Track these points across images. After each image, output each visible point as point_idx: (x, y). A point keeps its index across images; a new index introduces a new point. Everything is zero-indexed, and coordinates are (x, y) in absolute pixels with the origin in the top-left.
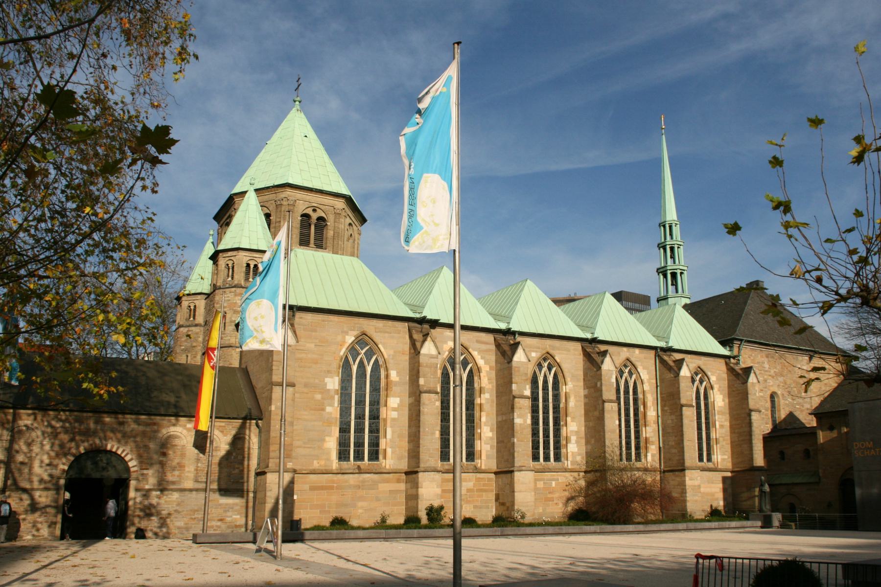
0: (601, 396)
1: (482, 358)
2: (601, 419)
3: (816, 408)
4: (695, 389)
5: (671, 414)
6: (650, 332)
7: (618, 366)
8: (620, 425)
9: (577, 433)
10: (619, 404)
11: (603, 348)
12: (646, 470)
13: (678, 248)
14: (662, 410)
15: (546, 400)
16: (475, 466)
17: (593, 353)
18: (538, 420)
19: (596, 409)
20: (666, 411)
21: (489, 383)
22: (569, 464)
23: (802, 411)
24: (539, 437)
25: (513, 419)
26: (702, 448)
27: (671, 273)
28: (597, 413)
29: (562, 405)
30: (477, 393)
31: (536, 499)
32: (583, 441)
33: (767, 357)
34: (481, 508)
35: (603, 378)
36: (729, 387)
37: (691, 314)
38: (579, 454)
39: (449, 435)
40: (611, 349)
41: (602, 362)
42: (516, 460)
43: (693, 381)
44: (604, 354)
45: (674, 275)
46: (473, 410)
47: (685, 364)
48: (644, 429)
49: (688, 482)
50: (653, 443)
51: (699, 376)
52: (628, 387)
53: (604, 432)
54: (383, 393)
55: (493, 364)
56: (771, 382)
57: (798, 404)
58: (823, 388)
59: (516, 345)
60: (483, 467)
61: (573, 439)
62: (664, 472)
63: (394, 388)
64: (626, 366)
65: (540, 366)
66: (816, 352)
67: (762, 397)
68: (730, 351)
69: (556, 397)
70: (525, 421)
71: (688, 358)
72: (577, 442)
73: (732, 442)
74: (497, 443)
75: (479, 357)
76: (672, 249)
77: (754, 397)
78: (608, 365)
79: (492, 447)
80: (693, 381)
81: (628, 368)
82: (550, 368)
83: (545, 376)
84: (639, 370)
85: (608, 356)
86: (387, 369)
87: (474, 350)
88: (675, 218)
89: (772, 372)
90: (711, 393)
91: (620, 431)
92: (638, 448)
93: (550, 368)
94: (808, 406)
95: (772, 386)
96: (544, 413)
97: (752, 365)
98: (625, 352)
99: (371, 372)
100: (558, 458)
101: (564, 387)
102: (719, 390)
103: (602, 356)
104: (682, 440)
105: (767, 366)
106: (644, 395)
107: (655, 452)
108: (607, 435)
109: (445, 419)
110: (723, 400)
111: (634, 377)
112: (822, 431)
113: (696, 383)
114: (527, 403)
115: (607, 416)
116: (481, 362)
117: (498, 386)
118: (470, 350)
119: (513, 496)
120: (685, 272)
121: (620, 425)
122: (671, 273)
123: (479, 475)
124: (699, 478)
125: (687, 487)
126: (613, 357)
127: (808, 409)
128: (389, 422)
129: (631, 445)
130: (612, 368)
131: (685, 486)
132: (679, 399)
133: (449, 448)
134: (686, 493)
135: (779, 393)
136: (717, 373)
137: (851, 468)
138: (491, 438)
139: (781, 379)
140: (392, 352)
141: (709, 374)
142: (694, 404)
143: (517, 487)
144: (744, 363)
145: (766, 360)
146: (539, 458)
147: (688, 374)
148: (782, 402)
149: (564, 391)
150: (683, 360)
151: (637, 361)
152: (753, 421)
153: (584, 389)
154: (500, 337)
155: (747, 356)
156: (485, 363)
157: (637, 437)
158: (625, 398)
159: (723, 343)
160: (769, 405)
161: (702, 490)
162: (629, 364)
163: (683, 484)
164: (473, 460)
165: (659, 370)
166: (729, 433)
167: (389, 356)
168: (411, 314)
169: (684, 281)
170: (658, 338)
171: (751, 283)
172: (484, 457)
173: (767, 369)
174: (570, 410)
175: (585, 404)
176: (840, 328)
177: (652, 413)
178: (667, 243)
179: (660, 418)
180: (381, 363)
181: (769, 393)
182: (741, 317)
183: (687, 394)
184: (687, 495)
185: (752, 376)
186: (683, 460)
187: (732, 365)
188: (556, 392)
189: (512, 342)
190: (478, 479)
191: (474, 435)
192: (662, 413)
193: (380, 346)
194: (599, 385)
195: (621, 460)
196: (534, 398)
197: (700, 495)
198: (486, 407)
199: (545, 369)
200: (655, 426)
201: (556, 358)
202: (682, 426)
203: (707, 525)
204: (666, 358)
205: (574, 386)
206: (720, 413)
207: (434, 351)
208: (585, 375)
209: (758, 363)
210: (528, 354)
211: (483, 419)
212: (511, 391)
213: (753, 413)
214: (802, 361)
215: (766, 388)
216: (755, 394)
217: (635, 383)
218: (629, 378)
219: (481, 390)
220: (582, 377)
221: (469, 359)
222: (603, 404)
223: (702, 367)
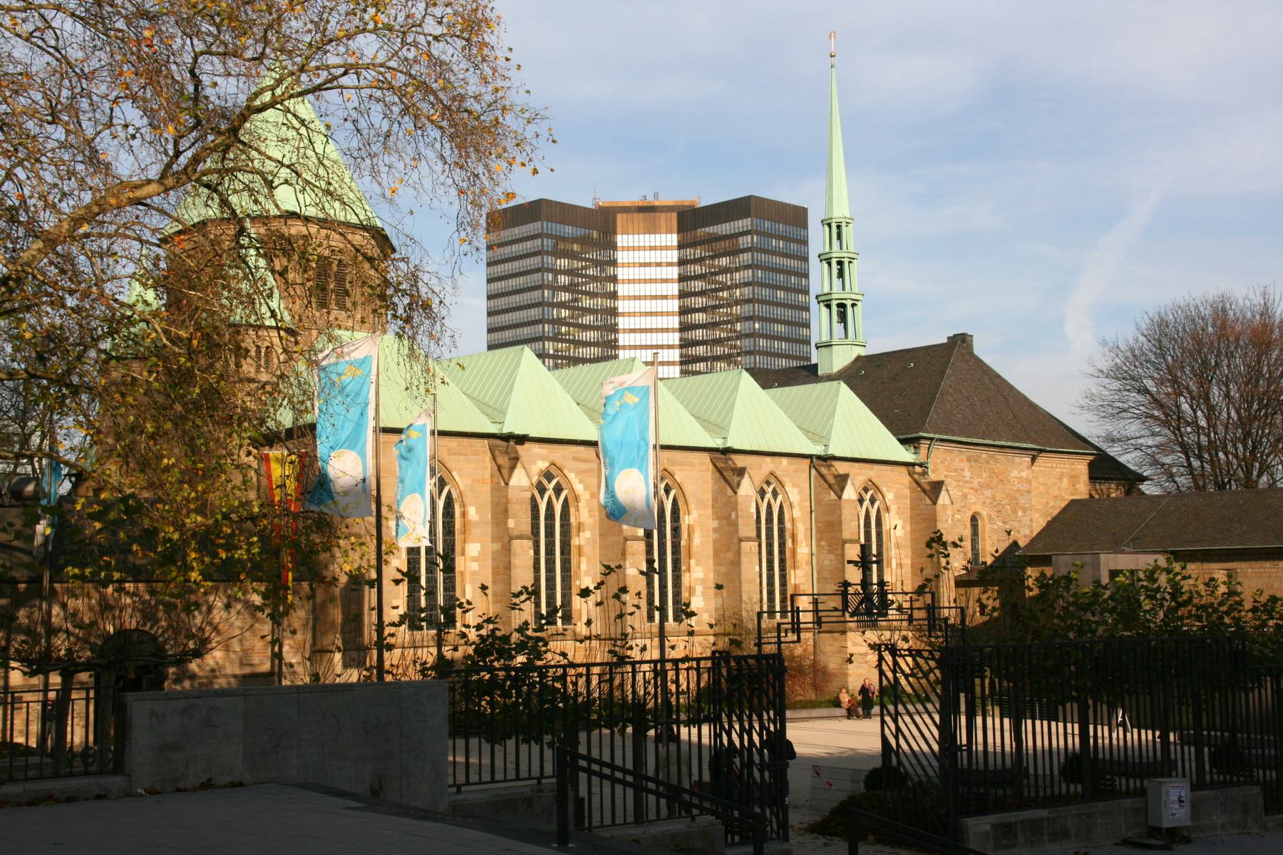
1: (581, 482)
5: (830, 552)
9: (703, 581)
14: (818, 545)
19: (729, 550)
20: (823, 547)
21: (590, 516)
28: (730, 555)
29: (683, 543)
33: (969, 460)
36: (912, 508)
46: (569, 554)
48: (792, 572)
54: (458, 537)
56: (972, 498)
58: (1052, 503)
61: (699, 589)
63: (473, 530)
64: (768, 483)
66: (1041, 451)
68: (915, 453)
69: (676, 531)
72: (703, 594)
75: (577, 480)
80: (861, 501)
81: (772, 487)
86: (463, 505)
87: (570, 471)
89: (975, 484)
94: (1027, 532)
95: (974, 503)
98: (768, 464)
99: (444, 508)
101: (687, 517)
102: (897, 513)
105: (967, 474)
106: (793, 524)
111: (780, 498)
113: (867, 503)
114: (641, 546)
116: (579, 488)
118: (565, 471)
127: (1025, 536)
128: (468, 577)
135: (984, 513)
136: (896, 489)
139: (988, 493)
140: (469, 482)
141: (884, 490)
144: (934, 471)
145: (966, 465)
148: (988, 527)
149: (687, 522)
151: (784, 475)
155: (939, 461)
156: (585, 489)
162: (772, 480)
167: (466, 486)
168: (493, 429)
170: (815, 442)
173: (967, 479)
174: (695, 549)
175: (715, 541)
177: (803, 550)
180: (454, 496)
181: (969, 515)
187: (916, 476)
188: (676, 524)
191: (570, 589)
193: (454, 474)
194: (733, 516)
200: (808, 568)
201: (676, 477)
204: (824, 471)
205: (700, 515)
208: (715, 500)
209: (955, 470)
211: (583, 567)
214: (1020, 464)
215: (964, 507)
217: (781, 507)
218: (772, 501)
220: (710, 503)
221: (564, 485)
223: (874, 480)
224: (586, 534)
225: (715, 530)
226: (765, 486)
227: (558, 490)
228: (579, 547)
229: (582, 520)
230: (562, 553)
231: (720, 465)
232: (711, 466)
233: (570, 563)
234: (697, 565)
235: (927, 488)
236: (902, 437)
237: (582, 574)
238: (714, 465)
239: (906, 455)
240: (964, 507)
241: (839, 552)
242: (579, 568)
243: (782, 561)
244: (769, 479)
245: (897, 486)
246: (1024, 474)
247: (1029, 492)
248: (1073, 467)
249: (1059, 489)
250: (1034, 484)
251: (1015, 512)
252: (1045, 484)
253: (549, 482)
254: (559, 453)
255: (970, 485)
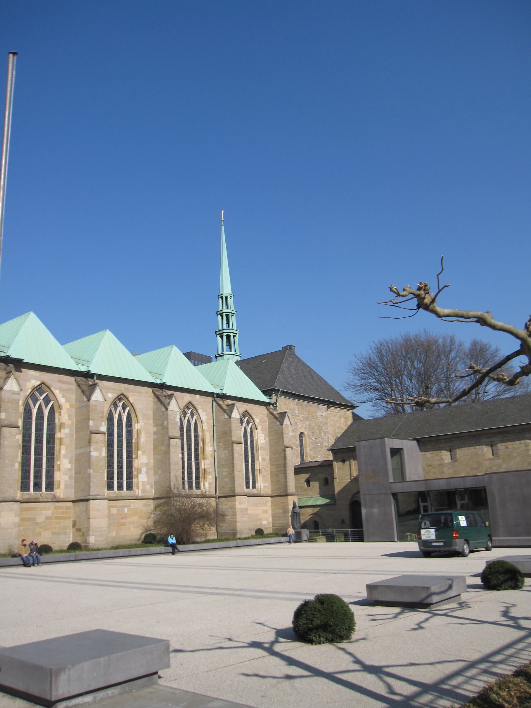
0: (168, 433)
1: (63, 396)
2: (167, 452)
3: (333, 445)
4: (243, 429)
5: (225, 449)
6: (208, 380)
7: (182, 407)
8: (183, 458)
10: (183, 440)
11: (169, 392)
12: (204, 496)
13: (232, 316)
14: (218, 446)
15: (120, 435)
16: (54, 496)
17: (161, 396)
18: (113, 453)
21: (69, 419)
22: (138, 492)
23: (322, 448)
24: (113, 468)
25: (90, 452)
26: (249, 477)
27: (226, 335)
28: (163, 448)
29: (134, 441)
30: (57, 428)
31: (109, 524)
32: (152, 472)
33: (297, 405)
34: (59, 534)
35: (169, 417)
37: (241, 368)
38: (149, 483)
39: (30, 466)
40: (176, 394)
41: (169, 404)
42: (91, 489)
43: (242, 422)
44: (170, 397)
45: (228, 337)
46: (54, 443)
47: (235, 407)
48: (203, 461)
49: (238, 506)
50: (210, 473)
51: (247, 418)
52: (190, 426)
53: (170, 464)
55: (73, 402)
56: (300, 424)
57: (320, 442)
58: (337, 431)
59: (94, 386)
60: (62, 496)
62: (219, 497)
64: (189, 409)
65: (115, 405)
67: (294, 436)
69: (130, 433)
70: (101, 454)
71: (238, 404)
72: (147, 473)
73: (271, 472)
74: (76, 474)
75: (61, 395)
76: (227, 316)
77: (288, 436)
78: (174, 407)
79: (70, 477)
80: (242, 422)
81: (190, 410)
82: (124, 408)
83: (120, 415)
84: (199, 412)
85: (174, 399)
87: (56, 389)
88: (231, 293)
90: (255, 433)
91: (183, 463)
92: (198, 478)
93: (124, 408)
94: (327, 444)
96: (118, 447)
97: (286, 410)
98: (188, 397)
100: (130, 487)
101: (136, 425)
102: (261, 430)
103: (169, 399)
104: (233, 471)
105: (297, 412)
106: (203, 433)
107: (211, 481)
108: (172, 467)
109: (26, 452)
110: (265, 439)
111: (195, 417)
112: (337, 462)
113: (244, 424)
114: (103, 438)
115: (172, 450)
116: (62, 400)
117: (77, 422)
118: (52, 389)
119: (89, 522)
120: (237, 335)
121: (183, 458)
122: (226, 335)
123: (57, 504)
124: (246, 502)
125: (237, 510)
126: (178, 400)
127: (326, 446)
129: (192, 475)
130: (177, 409)
131: (236, 509)
132: (231, 436)
133: (29, 478)
134: (236, 515)
135: (306, 433)
137: (358, 492)
138: (70, 470)
141: (254, 417)
142: (243, 441)
143: (92, 514)
144: (280, 409)
146: (113, 487)
147: (238, 417)
148: (308, 440)
149: (137, 428)
150: (234, 404)
152: (287, 455)
153: (154, 427)
154: (80, 379)
156: (66, 401)
157: (197, 468)
158: (187, 435)
159: (265, 393)
160: (298, 442)
161: (249, 512)
162: (191, 406)
163: (233, 508)
164: (52, 490)
165: (215, 412)
166: (269, 465)
169: (236, 342)
170: (215, 386)
171: (286, 347)
172: (62, 486)
173: (297, 414)
175: (154, 440)
176: (349, 384)
178: (224, 311)
179: (215, 453)
181: (298, 433)
182: (278, 372)
183: (238, 433)
184: (237, 517)
185: (286, 418)
186: (234, 487)
187: (271, 410)
188: (129, 429)
189: (91, 383)
190: (56, 508)
191: (53, 467)
192: (217, 448)
194: (165, 424)
195: (184, 488)
196: (110, 434)
197: (247, 516)
198: (66, 441)
199: (120, 408)
201: (130, 399)
202: (233, 459)
203: (253, 541)
204: (221, 402)
205: (145, 424)
206: (263, 449)
207: (16, 388)
208: (154, 415)
209: (291, 409)
210: (105, 394)
211: (63, 452)
212: (88, 426)
213: (287, 449)
214: (322, 409)
215: (296, 429)
216: (288, 434)
217: (196, 423)
218: (191, 419)
219: (62, 426)
220: (152, 416)
221: (51, 396)
222: (169, 440)
223: (249, 411)
224: (67, 431)
225: (155, 433)
226: (186, 410)
227: (47, 400)
228: (61, 439)
229: (63, 421)
230: (48, 442)
231: (157, 393)
232: (152, 395)
233: (54, 450)
234: (143, 455)
235: (277, 416)
236: (261, 390)
237: (62, 457)
238: (154, 394)
239: (265, 399)
240: (296, 429)
241: (230, 449)
242: (60, 453)
243: (197, 455)
244: (189, 405)
245: (261, 415)
246: (324, 414)
247: (327, 424)
248: (345, 413)
249: (340, 423)
250: (329, 420)
251: (320, 433)
252: (333, 420)
253: (41, 395)
254: (48, 377)
255: (298, 418)
